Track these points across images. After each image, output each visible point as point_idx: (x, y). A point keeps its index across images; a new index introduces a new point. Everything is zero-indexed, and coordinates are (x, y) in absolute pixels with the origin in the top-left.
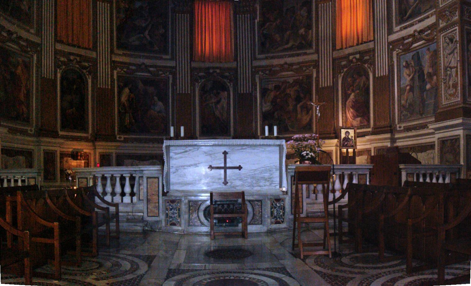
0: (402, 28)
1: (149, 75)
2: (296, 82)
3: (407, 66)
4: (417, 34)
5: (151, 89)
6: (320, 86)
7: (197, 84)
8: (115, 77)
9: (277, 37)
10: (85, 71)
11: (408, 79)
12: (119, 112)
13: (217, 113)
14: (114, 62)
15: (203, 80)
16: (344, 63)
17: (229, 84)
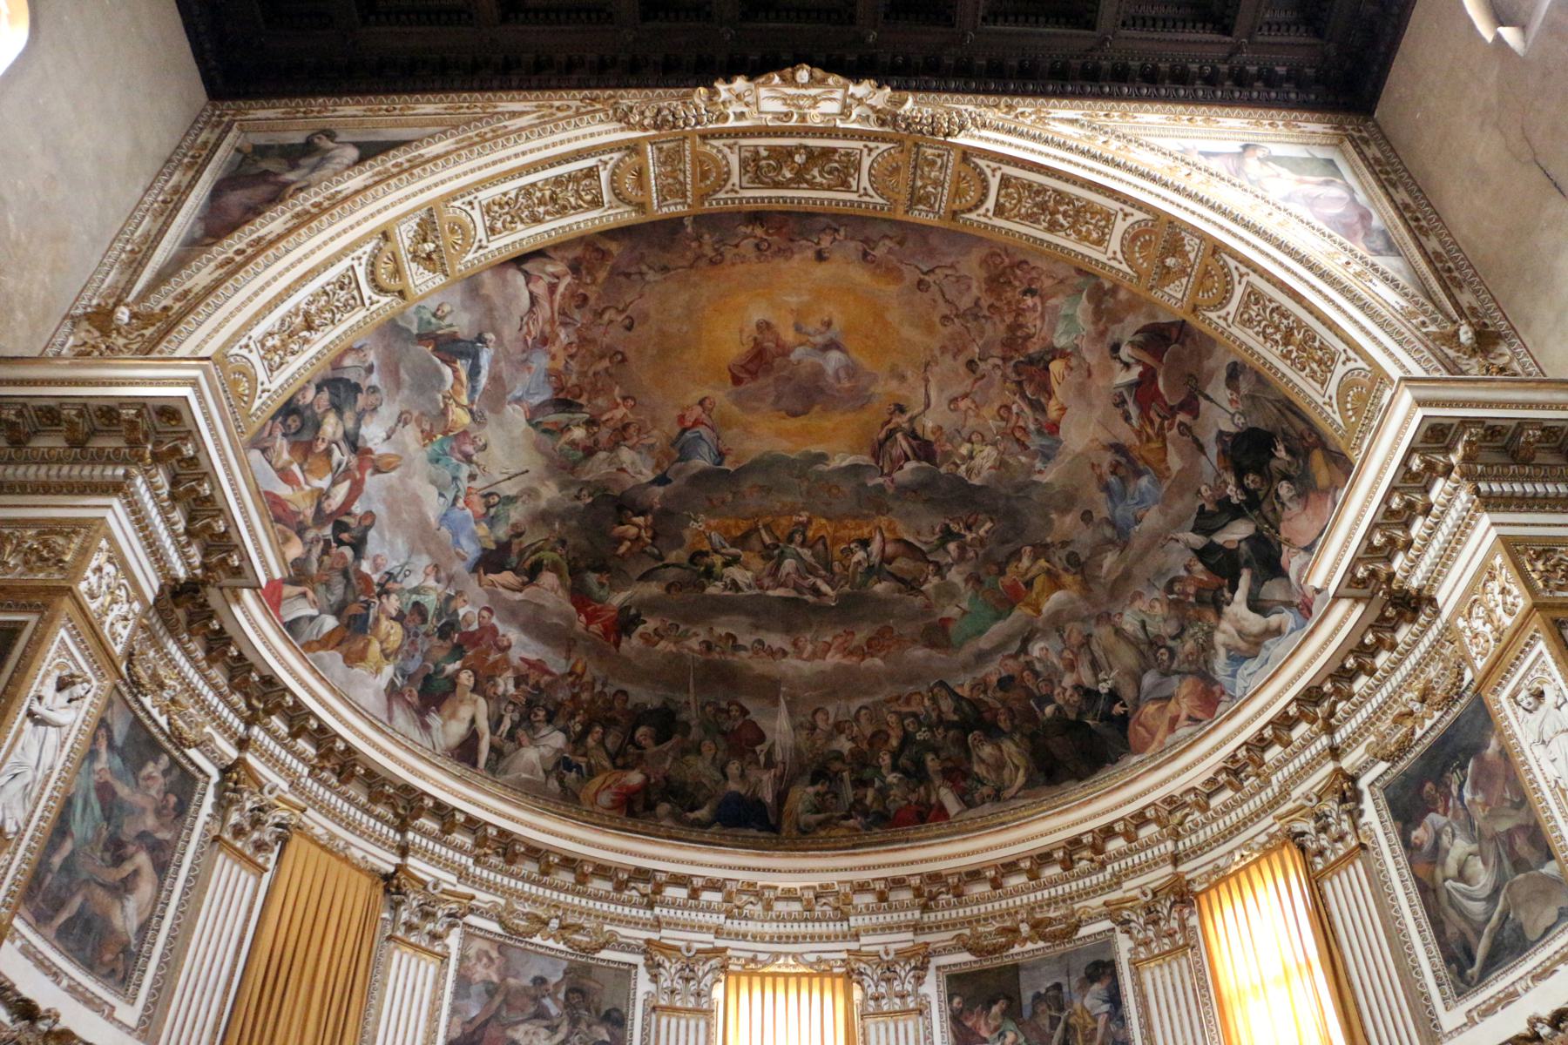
0: (1475, 1014)
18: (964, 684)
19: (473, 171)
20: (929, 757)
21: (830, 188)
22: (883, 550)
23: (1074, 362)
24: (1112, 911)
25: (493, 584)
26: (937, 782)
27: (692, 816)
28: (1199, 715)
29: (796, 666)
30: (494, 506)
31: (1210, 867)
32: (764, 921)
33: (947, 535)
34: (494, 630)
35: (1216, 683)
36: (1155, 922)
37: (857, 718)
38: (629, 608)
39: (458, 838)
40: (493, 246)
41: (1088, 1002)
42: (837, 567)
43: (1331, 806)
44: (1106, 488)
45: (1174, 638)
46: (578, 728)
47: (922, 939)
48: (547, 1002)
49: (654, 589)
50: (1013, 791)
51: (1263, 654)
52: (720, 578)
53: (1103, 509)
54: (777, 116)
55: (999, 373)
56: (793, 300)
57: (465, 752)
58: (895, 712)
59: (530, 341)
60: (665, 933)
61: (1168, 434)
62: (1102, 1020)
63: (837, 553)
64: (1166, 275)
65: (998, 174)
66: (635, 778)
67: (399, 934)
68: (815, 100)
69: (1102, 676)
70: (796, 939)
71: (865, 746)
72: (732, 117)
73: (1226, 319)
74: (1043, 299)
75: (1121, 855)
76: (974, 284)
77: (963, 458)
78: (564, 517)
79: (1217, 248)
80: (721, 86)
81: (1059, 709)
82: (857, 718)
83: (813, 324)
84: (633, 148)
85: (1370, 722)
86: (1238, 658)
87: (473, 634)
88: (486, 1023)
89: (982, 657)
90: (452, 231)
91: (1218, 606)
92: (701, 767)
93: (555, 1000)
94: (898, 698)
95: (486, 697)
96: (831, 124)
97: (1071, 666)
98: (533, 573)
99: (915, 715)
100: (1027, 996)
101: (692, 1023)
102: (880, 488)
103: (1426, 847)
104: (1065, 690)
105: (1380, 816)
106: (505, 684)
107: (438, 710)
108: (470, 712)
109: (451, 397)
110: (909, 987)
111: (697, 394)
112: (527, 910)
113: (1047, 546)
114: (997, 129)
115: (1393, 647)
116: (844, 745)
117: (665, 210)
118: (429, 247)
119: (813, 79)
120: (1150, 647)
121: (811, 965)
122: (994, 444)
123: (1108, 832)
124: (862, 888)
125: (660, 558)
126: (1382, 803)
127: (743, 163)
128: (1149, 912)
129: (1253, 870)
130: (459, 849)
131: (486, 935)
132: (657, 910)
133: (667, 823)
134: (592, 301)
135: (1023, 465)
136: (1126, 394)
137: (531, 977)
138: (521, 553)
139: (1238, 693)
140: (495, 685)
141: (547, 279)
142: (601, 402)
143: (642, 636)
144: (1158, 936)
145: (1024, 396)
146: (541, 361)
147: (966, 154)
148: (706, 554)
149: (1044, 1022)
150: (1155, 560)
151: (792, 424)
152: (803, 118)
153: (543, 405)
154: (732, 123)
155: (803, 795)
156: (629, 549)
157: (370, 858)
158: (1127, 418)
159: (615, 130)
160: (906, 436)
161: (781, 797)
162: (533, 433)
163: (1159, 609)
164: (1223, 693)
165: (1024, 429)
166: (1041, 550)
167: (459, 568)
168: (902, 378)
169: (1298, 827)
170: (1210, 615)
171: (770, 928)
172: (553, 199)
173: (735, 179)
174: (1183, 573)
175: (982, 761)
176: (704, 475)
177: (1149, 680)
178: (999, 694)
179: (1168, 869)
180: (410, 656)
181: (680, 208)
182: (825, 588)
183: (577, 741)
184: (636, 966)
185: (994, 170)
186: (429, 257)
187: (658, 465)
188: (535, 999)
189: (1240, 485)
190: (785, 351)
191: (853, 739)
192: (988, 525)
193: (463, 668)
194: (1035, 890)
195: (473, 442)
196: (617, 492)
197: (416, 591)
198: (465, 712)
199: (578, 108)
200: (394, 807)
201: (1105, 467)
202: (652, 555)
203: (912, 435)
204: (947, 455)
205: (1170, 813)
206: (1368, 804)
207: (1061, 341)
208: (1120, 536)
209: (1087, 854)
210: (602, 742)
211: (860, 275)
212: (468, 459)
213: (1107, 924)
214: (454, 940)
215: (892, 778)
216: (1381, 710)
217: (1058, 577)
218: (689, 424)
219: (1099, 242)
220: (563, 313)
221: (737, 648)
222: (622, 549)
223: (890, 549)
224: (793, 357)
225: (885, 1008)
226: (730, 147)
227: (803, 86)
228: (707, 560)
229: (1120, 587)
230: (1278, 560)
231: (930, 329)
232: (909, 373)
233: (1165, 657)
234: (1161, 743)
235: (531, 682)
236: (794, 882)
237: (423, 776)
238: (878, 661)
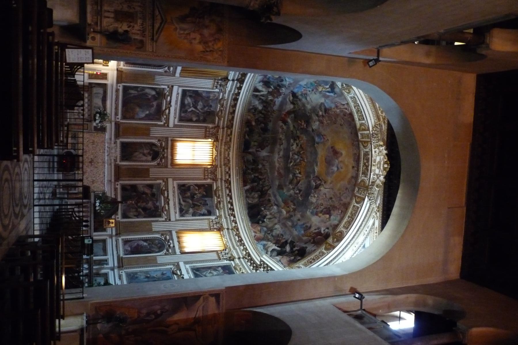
1: (164, 108)
2: (157, 208)
3: (163, 274)
4: (182, 276)
5: (153, 110)
6: (153, 223)
7: (157, 140)
9: (189, 194)
10: (167, 68)
11: (155, 275)
12: (137, 87)
13: (137, 154)
14: (172, 86)
15: (159, 145)
16: (168, 237)
17: (156, 162)
18: (270, 192)
19: (360, 94)
20: (256, 184)
21: (362, 170)
22: (298, 177)
23: (328, 220)
24: (220, 216)
25: (290, 95)
26: (251, 185)
27: (246, 135)
28: (256, 237)
29: (276, 156)
30: (305, 95)
31: (225, 235)
32: (224, 149)
33: (300, 191)
34: (280, 95)
35: (261, 241)
36: (216, 224)
37: (265, 169)
38: (288, 123)
40: (349, 98)
41: (204, 210)
42: (296, 167)
43: (229, 255)
44: (304, 224)
45: (272, 234)
46: (263, 112)
47: (219, 180)
48: (207, 108)
49: (292, 128)
50: (247, 200)
51: (264, 250)
52: (294, 142)
53: (300, 223)
54: (375, 160)
55: (329, 204)
56: (346, 160)
57: (256, 90)
58: (266, 177)
59: (336, 104)
60: (221, 130)
61: (310, 237)
62: (200, 212)
63: (298, 167)
64: (333, 239)
65: (360, 206)
66: (254, 123)
67: (216, 81)
68: (379, 168)
69: (268, 220)
70: (220, 155)
71: (259, 171)
72: (375, 150)
73: (322, 249)
74: (340, 214)
75: (230, 219)
76: (345, 200)
77: (314, 195)
78: (305, 110)
79: (334, 248)
80: (383, 148)
81: (263, 211)
82: (265, 169)
83: (341, 165)
84: (369, 130)
85: (243, 265)
86: (264, 246)
87: (279, 91)
89: (275, 196)
90: (348, 90)
91: (275, 243)
92: (256, 137)
93: (208, 109)
94: (268, 178)
95: (267, 94)
96: (372, 171)
97: (271, 214)
98: (292, 103)
99: (265, 182)
100: (206, 199)
101: (203, 135)
102: (310, 177)
103: (217, 269)
104: (266, 212)
105: (225, 263)
106: (270, 98)
107: (263, 85)
108: (264, 91)
109: (324, 88)
110: (209, 177)
111: (329, 138)
112: (225, 103)
113: (295, 211)
114: (369, 207)
115: (253, 269)
116: (260, 166)
117: (359, 134)
118: (344, 86)
119: (385, 169)
120: (271, 230)
121: (215, 158)
122: (316, 202)
123: (234, 217)
124: (229, 169)
125: (298, 130)
126: (228, 264)
127: (367, 152)
128: (218, 223)
129: (222, 241)
130: (234, 91)
131: (219, 96)
132: (226, 128)
133: (245, 130)
134: (345, 117)
135: (311, 207)
136: (319, 230)
138: (296, 101)
139: (258, 245)
140: (270, 96)
141: (348, 108)
142: (327, 118)
143: (282, 125)
144: (214, 224)
145: (324, 209)
146: (333, 106)
147: (364, 200)
148: (299, 139)
149: (200, 202)
150: (288, 233)
151: (324, 159)
152: (373, 165)
153: (325, 106)
154: (373, 150)
155: (250, 158)
156: (299, 123)
157: (230, 75)
158: (315, 230)
159: (372, 124)
160: (320, 183)
161: (250, 153)
162: (320, 104)
163: (278, 232)
164: (259, 242)
165: (318, 209)
166: (294, 210)
167: (292, 88)
168: (331, 183)
169: (227, 250)
170: (274, 242)
171: (223, 150)
172: (359, 111)
173: (365, 150)
174: (284, 238)
175: (254, 195)
176: (314, 140)
177: (265, 229)
178: (267, 199)
179: (226, 227)
180: (273, 79)
181: (360, 138)
182: (291, 164)
183: (260, 112)
184: (215, 124)
185: (360, 205)
186: (343, 85)
187: (316, 130)
188: (207, 106)
189: (297, 250)
190: (337, 158)
191: (261, 168)
192: (301, 199)
193: (273, 89)
194: (226, 202)
195: (316, 92)
196: (310, 121)
197: (286, 80)
198: (264, 90)
199: (382, 116)
200: (241, 78)
201: (307, 224)
202: (298, 128)
203: (320, 185)
204: (315, 192)
205: (236, 229)
206: (228, 262)
207: (332, 217)
208: (294, 226)
209: (232, 213)
210: (261, 117)
211: (349, 175)
212: (313, 90)
213: (218, 215)
214: (217, 90)
215: (253, 176)
216: (244, 267)
217: (289, 213)
218: (324, 136)
219: (344, 226)
220: (342, 111)
221: (280, 145)
222: (299, 122)
223: (298, 178)
224: (336, 160)
225: (206, 172)
226: (370, 149)
227: (383, 166)
228: (297, 139)
229: (284, 225)
230: (280, 255)
231: (339, 190)
232: (331, 185)
233: (269, 232)
234: (252, 230)
235: (272, 103)
236: (231, 156)
238: (276, 174)
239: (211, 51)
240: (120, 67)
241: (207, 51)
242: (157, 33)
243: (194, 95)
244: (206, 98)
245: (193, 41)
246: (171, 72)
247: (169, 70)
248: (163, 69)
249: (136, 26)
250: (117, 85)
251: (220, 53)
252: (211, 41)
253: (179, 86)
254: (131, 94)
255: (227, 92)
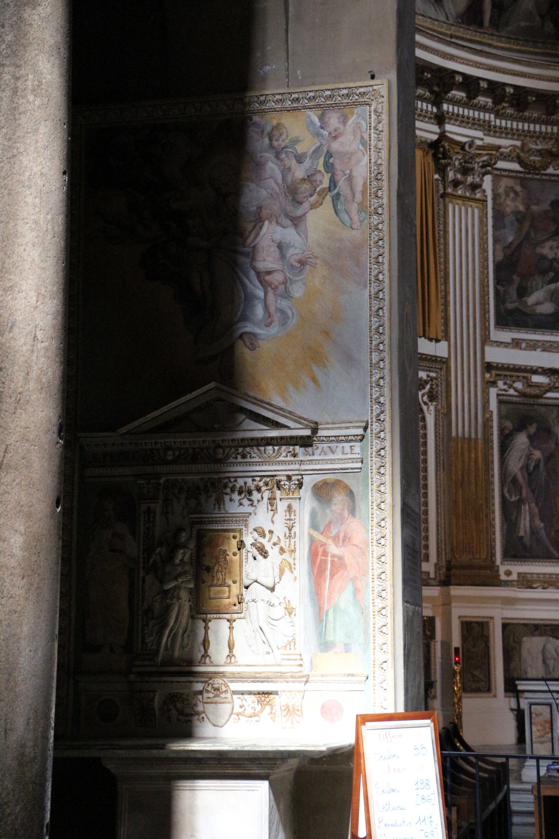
8: (493, 405)
12: (504, 501)
14: (489, 367)
39: (482, 100)
67: (449, 190)
88: (520, 246)
112: (540, 147)
130: (483, 108)
137: (549, 202)
214: (487, 182)
237: (452, 58)
239: (329, 167)
240: (432, 575)
241: (333, 183)
242: (277, 425)
243: (515, 277)
244: (525, 230)
245: (293, 254)
246: (433, 375)
247: (426, 382)
248: (425, 408)
249: (253, 522)
250: (506, 584)
251: (334, 120)
252: (286, 171)
253: (486, 340)
254: (534, 531)
255: (490, 140)
